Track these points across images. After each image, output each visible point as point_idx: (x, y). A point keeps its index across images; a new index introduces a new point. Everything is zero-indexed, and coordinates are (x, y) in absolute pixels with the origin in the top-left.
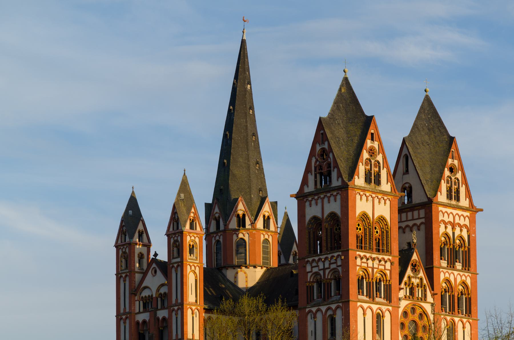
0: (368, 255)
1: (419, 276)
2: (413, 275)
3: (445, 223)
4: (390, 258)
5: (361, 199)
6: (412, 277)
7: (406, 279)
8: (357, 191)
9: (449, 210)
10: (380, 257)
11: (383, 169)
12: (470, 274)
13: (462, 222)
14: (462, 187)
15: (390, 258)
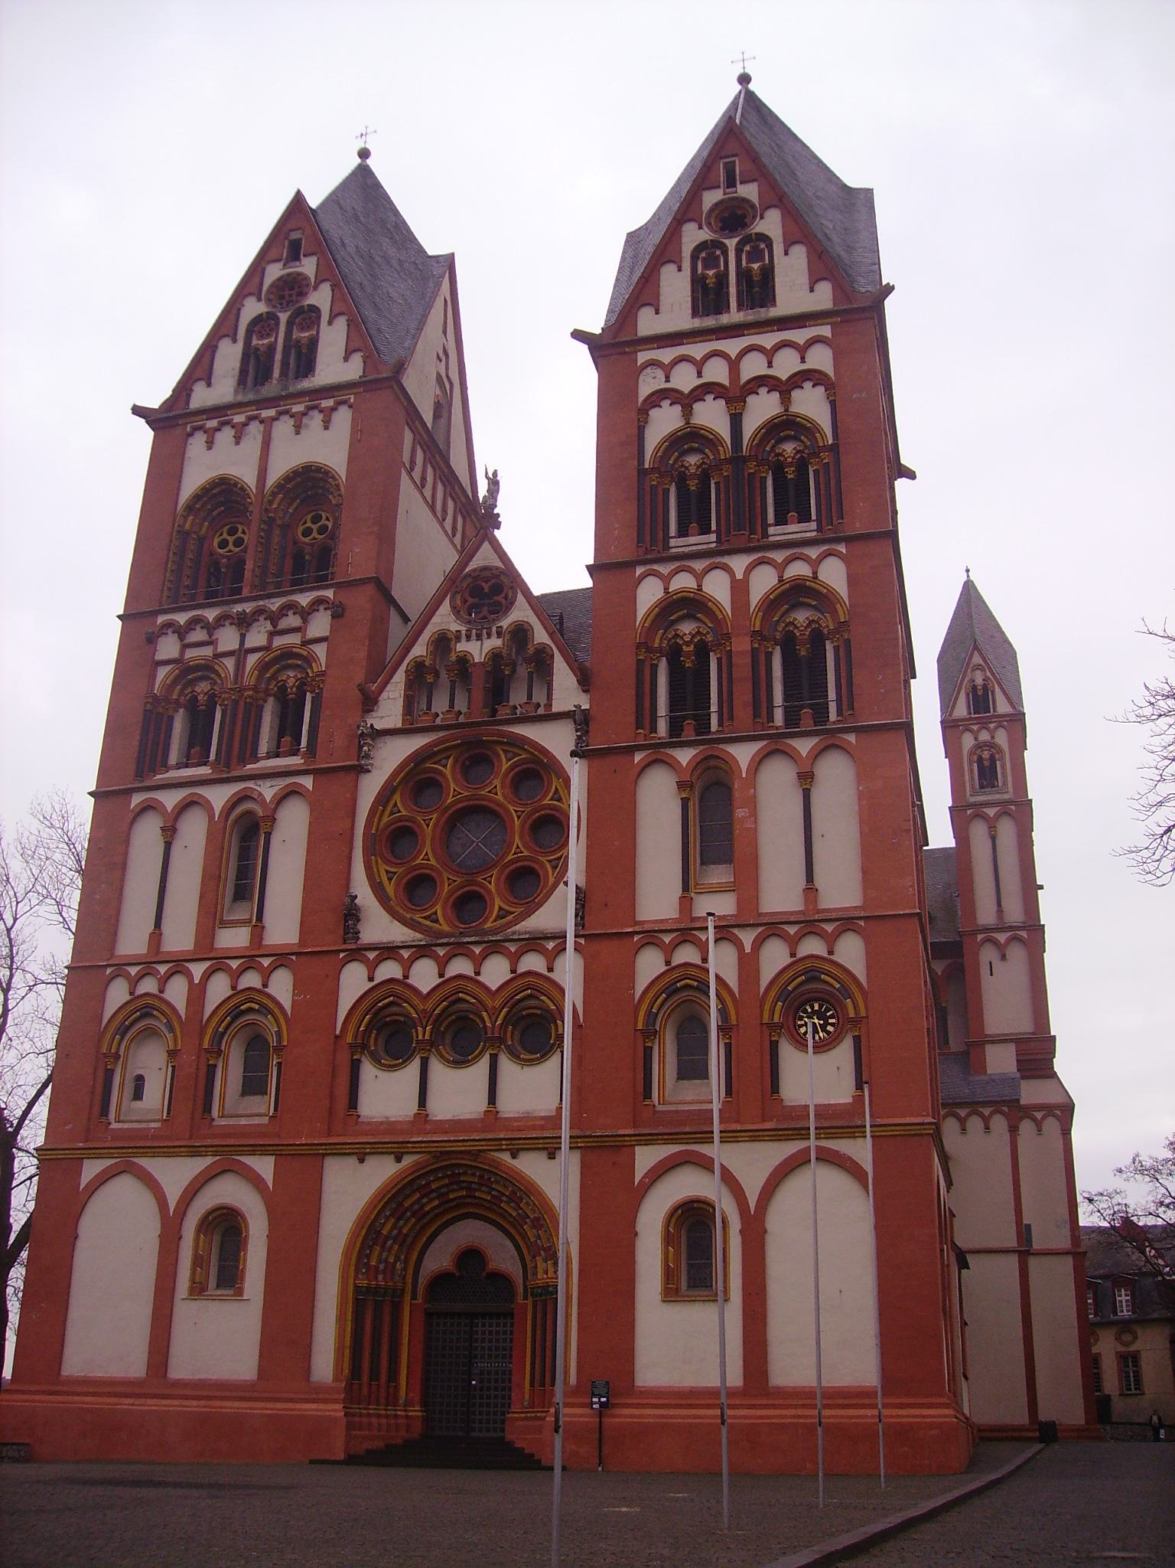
0: (211, 614)
1: (505, 623)
2: (463, 629)
3: (687, 401)
4: (329, 593)
5: (210, 444)
6: (458, 638)
7: (419, 650)
8: (189, 426)
9: (698, 350)
10: (275, 604)
11: (330, 323)
12: (843, 545)
13: (786, 365)
14: (786, 253)
15: (329, 593)
